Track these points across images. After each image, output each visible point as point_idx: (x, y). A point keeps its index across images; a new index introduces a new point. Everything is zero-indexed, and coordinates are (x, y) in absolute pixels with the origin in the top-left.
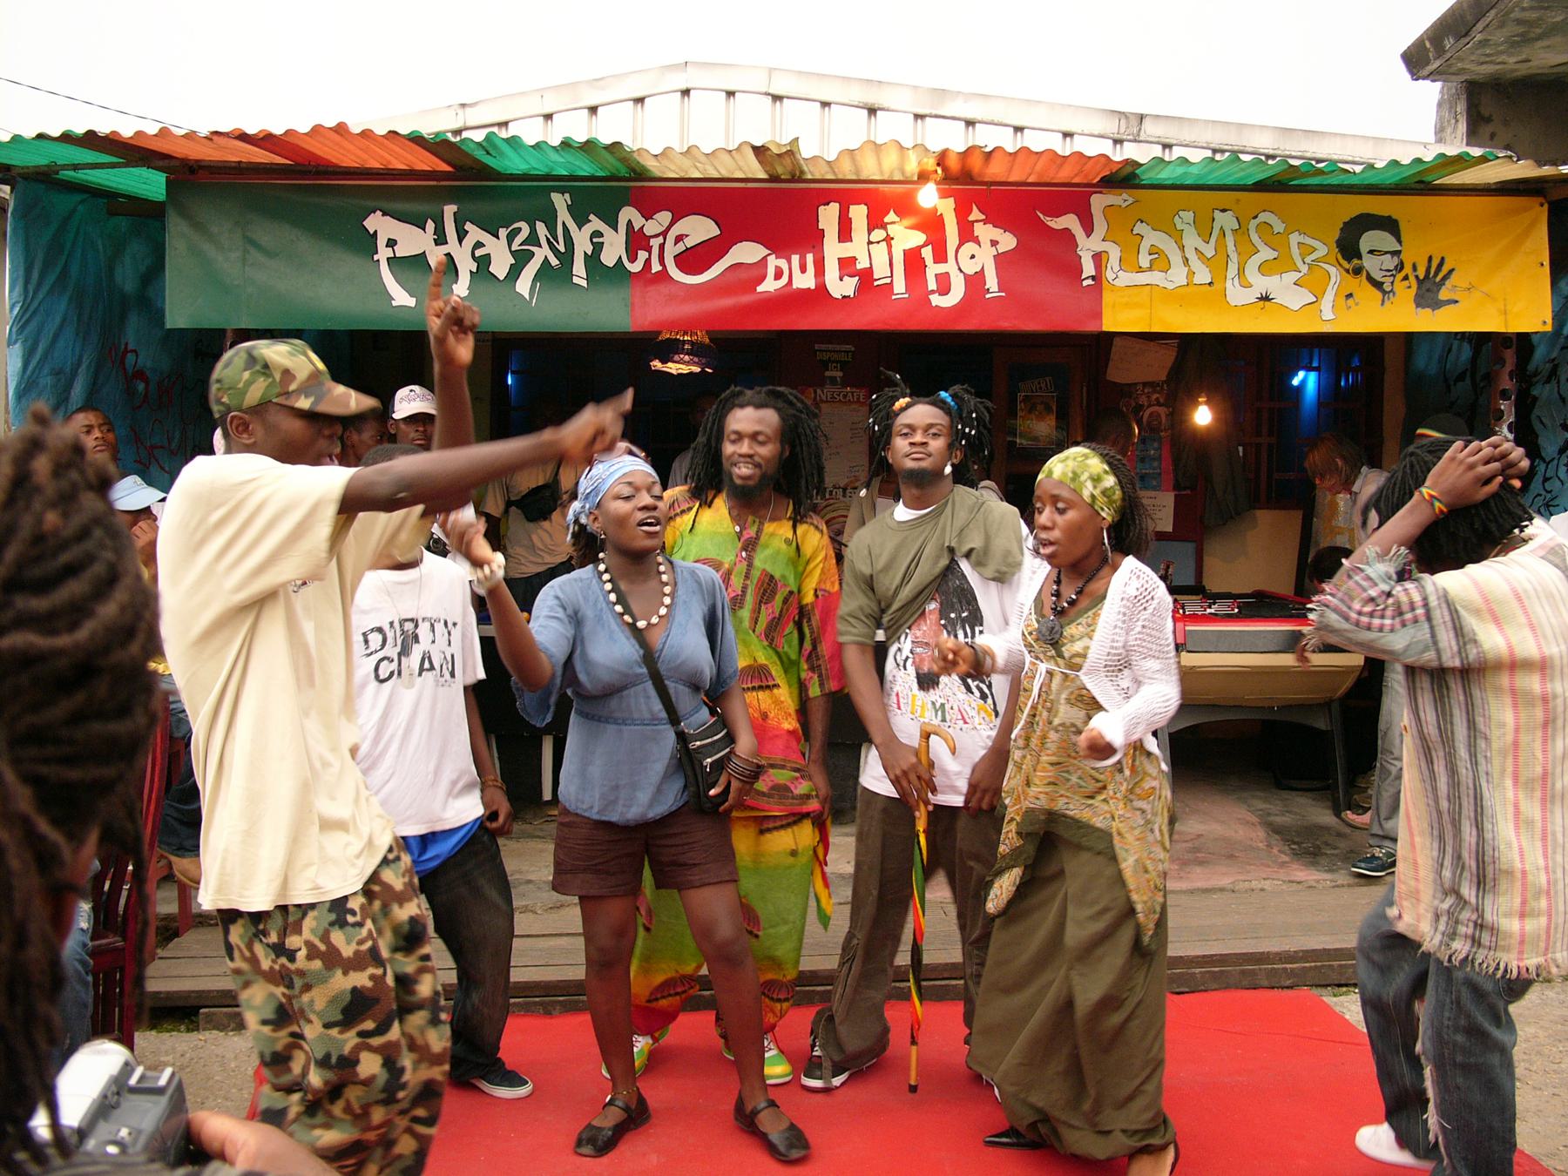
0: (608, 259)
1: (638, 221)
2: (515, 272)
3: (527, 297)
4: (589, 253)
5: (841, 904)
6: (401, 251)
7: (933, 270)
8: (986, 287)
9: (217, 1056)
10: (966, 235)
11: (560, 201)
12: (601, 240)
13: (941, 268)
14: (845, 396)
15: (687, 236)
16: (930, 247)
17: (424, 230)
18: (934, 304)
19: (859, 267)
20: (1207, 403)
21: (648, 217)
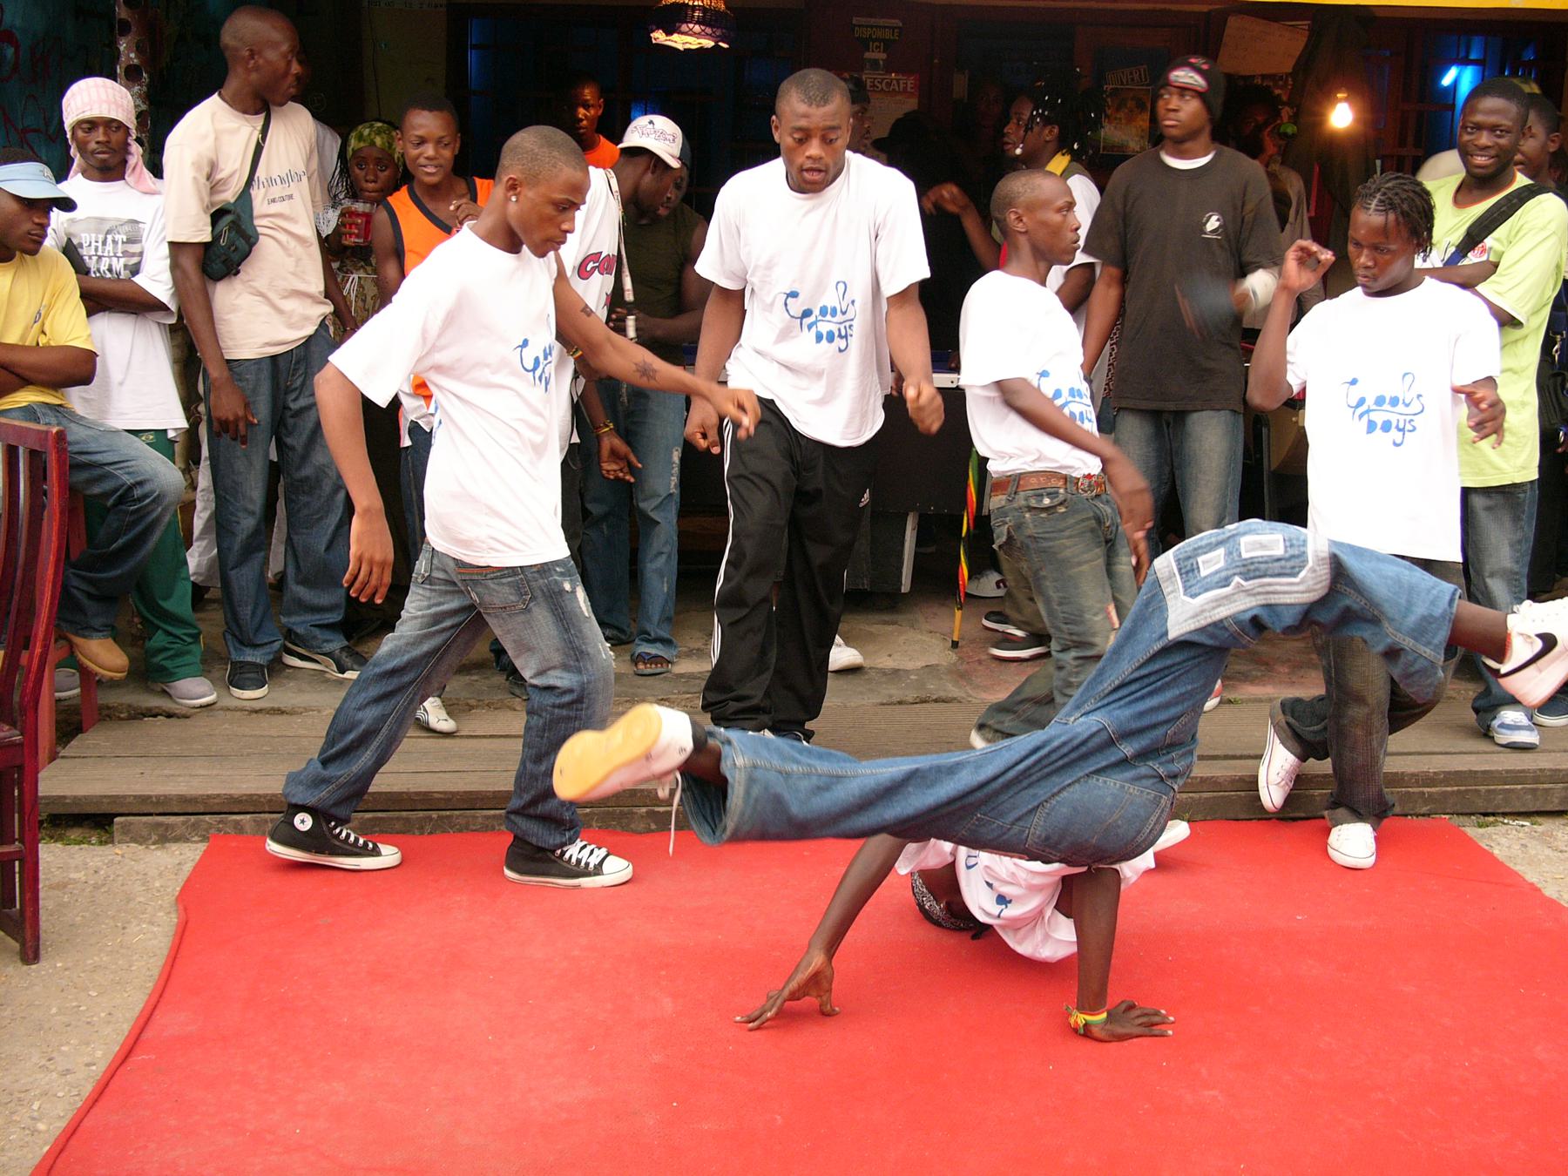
5: (883, 704)
9: (138, 873)
20: (1346, 100)
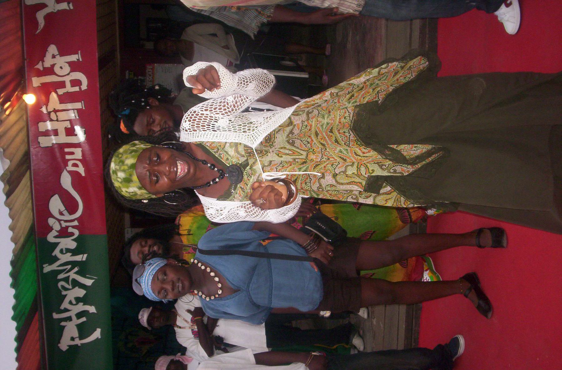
0: (73, 245)
1: (54, 233)
2: (82, 286)
3: (93, 281)
4: (71, 254)
6: (76, 334)
7: (69, 88)
8: (76, 61)
10: (50, 71)
11: (47, 269)
12: (64, 249)
13: (68, 84)
14: (150, 75)
15: (59, 210)
16: (58, 90)
17: (64, 327)
18: (86, 88)
19: (69, 126)
21: (51, 229)
